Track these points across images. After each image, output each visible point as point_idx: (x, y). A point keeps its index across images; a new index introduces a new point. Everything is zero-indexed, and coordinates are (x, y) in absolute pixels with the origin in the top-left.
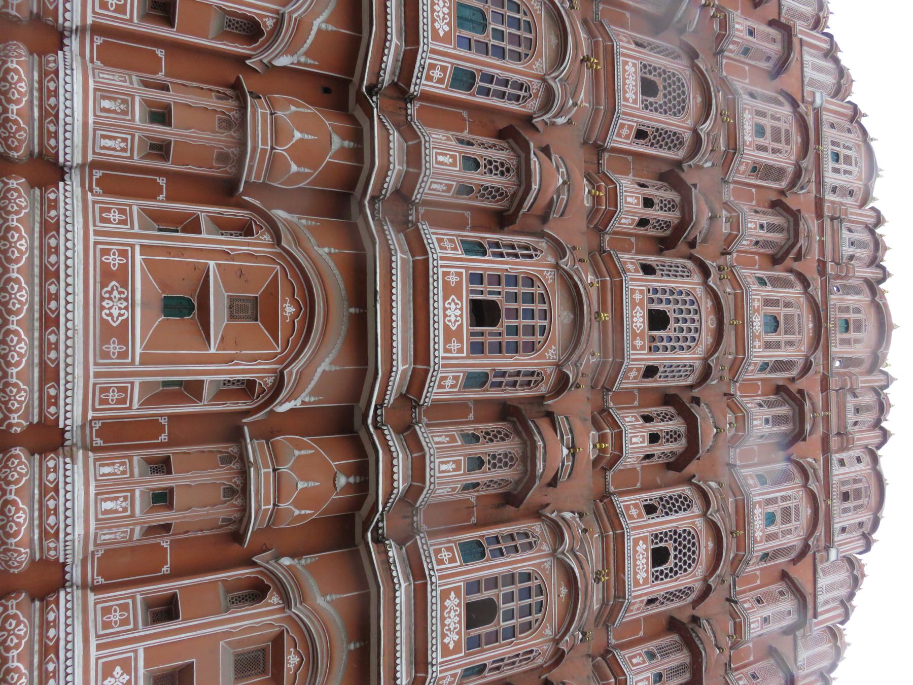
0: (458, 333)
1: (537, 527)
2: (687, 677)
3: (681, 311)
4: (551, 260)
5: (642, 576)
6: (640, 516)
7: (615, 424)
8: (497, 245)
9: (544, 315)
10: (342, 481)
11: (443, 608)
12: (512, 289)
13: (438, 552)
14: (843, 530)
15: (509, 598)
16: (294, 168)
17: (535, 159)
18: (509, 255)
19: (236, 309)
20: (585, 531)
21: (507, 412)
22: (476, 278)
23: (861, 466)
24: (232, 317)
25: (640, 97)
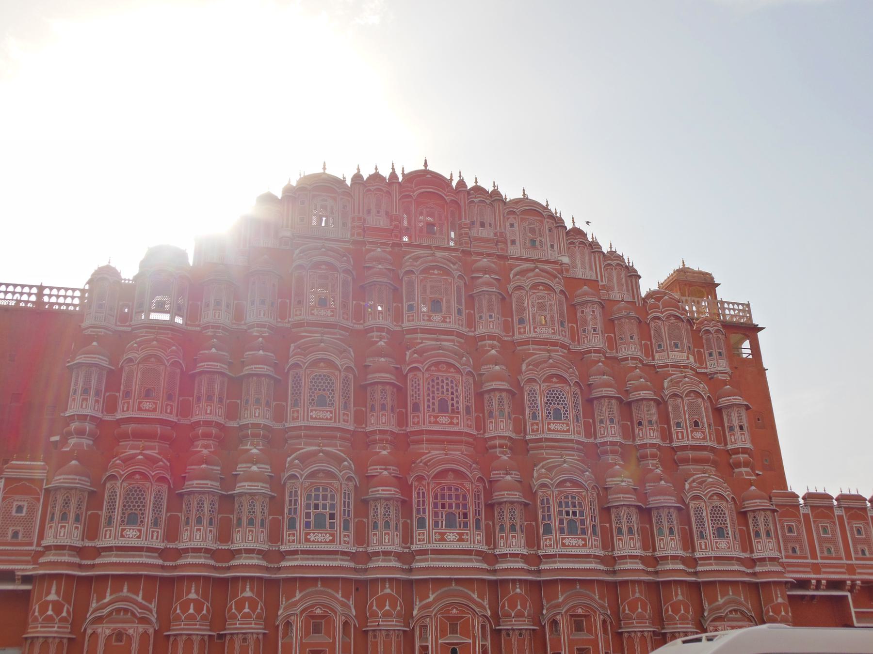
0: (460, 535)
1: (540, 493)
2: (614, 401)
3: (438, 390)
4: (424, 482)
5: (565, 428)
6: (537, 424)
7: (494, 438)
8: (418, 510)
9: (450, 489)
10: (518, 590)
11: (569, 546)
12: (440, 506)
13: (546, 546)
14: (552, 246)
15: (568, 513)
16: (399, 608)
17: (380, 488)
18: (424, 505)
19: (454, 631)
20: (543, 467)
21: (490, 507)
22: (436, 524)
23: (516, 225)
24: (457, 633)
25: (328, 409)
